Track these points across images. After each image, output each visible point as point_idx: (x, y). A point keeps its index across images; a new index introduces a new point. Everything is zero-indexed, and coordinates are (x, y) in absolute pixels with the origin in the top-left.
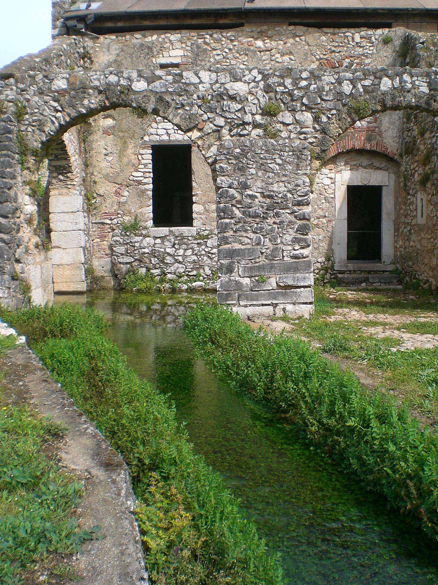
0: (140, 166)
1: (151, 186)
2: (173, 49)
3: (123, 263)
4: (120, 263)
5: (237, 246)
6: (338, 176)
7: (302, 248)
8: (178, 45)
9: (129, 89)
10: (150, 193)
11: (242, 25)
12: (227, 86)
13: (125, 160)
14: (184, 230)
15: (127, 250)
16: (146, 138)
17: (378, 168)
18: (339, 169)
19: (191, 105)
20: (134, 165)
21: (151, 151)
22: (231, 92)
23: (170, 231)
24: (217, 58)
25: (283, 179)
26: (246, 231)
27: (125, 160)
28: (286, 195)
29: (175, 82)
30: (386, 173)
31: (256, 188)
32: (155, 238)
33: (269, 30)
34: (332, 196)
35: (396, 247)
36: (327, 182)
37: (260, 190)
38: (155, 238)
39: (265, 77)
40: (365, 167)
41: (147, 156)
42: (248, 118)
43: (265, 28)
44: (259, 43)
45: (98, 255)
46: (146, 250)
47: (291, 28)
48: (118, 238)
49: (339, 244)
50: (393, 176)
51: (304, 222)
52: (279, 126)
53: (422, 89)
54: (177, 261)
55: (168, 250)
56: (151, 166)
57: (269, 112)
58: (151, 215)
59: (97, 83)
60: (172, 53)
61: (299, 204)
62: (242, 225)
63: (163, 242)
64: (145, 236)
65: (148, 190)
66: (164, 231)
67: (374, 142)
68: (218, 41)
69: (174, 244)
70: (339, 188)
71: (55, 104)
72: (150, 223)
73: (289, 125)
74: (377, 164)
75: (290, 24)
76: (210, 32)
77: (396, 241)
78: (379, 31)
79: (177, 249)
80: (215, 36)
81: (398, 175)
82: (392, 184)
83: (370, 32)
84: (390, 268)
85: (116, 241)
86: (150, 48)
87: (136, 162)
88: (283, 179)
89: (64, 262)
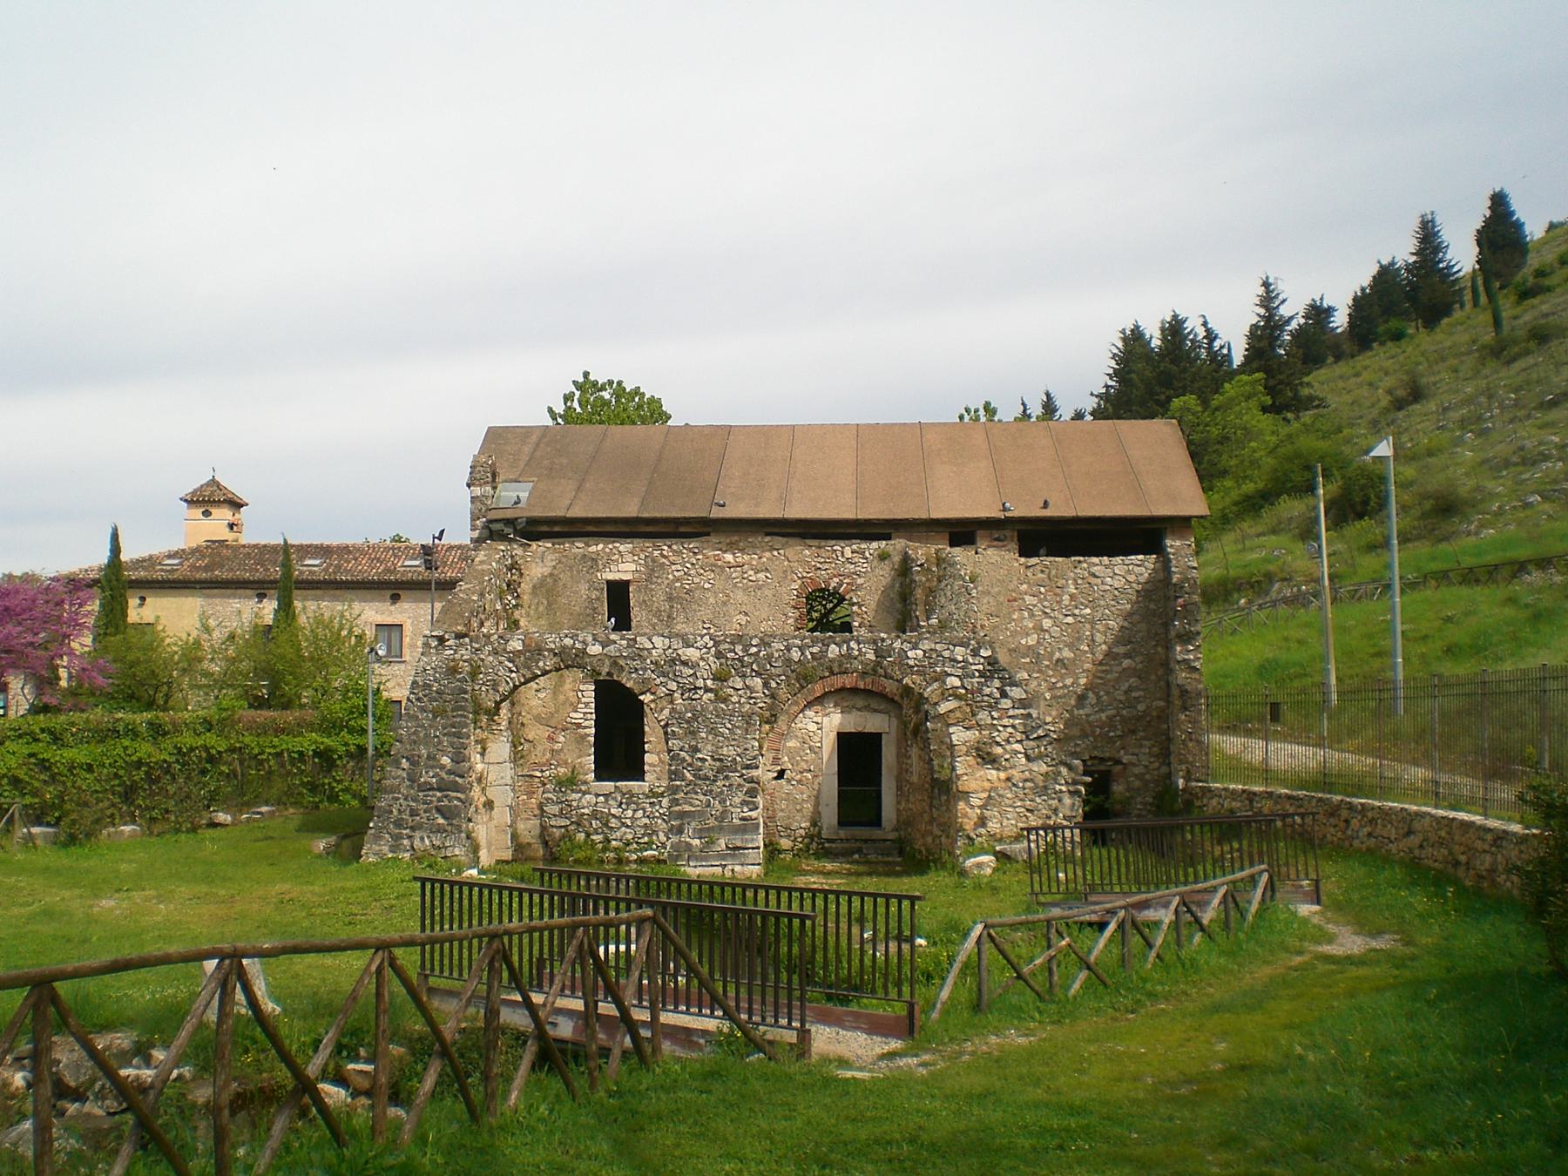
1: (593, 731)
5: (687, 808)
8: (629, 557)
9: (584, 652)
10: (592, 739)
11: (708, 534)
13: (562, 697)
17: (876, 711)
19: (645, 669)
27: (562, 697)
29: (629, 646)
30: (886, 717)
32: (597, 795)
38: (597, 795)
39: (716, 644)
41: (589, 692)
42: (700, 683)
44: (729, 557)
45: (524, 816)
46: (586, 811)
47: (767, 539)
50: (895, 722)
57: (720, 678)
61: (748, 767)
62: (692, 788)
64: (584, 793)
72: (592, 776)
74: (874, 705)
75: (767, 534)
77: (899, 803)
78: (875, 545)
81: (899, 717)
82: (894, 729)
84: (892, 836)
87: (575, 700)
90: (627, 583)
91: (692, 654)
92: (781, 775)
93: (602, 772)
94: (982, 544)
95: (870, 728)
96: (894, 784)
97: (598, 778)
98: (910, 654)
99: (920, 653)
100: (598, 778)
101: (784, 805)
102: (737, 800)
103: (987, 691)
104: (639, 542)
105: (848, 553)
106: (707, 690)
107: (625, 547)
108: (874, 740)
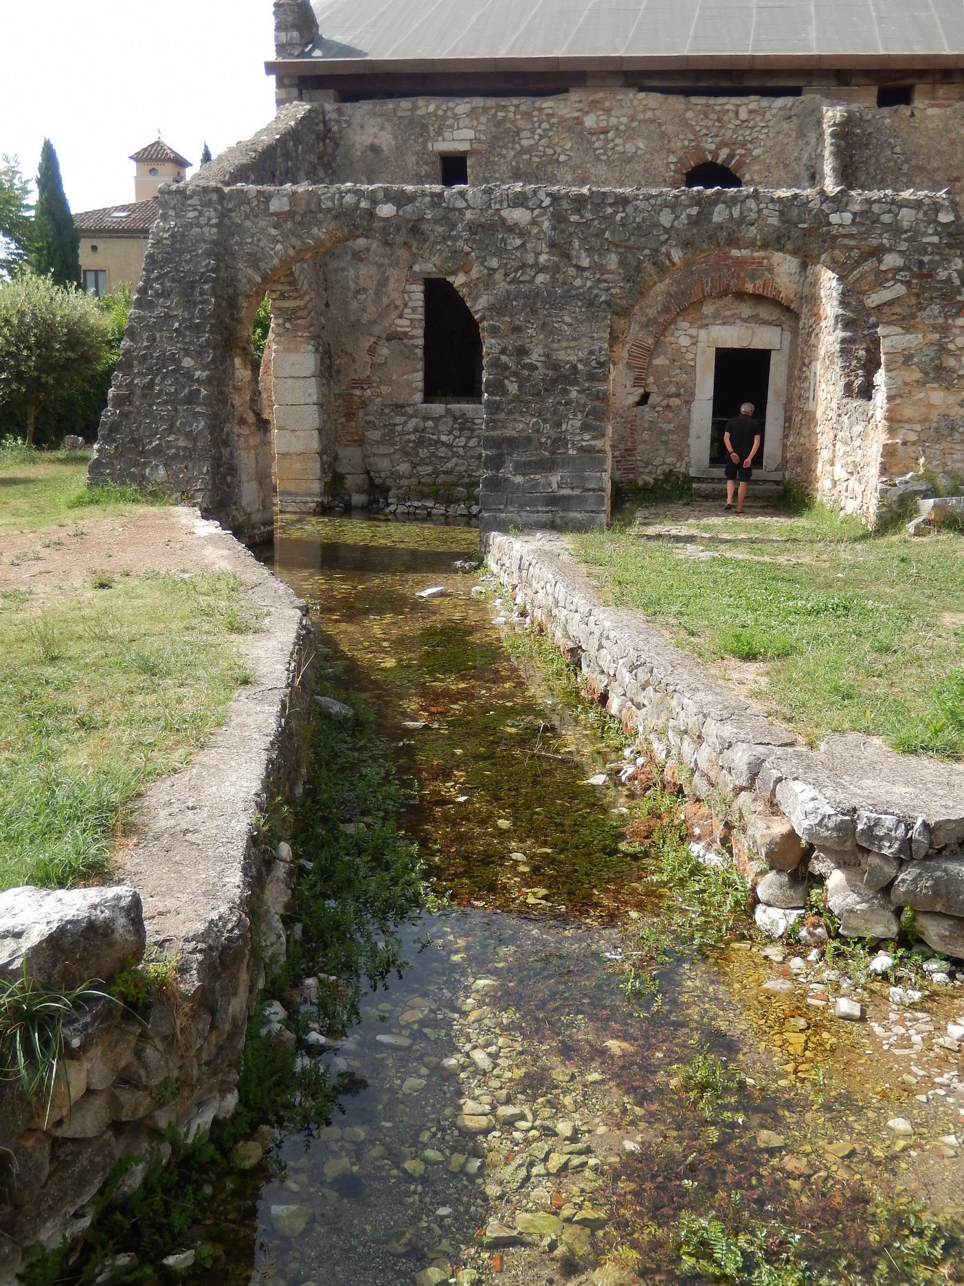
0: (407, 311)
1: (421, 342)
2: (458, 128)
3: (378, 455)
4: (375, 455)
6: (703, 333)
7: (594, 438)
8: (467, 121)
9: (371, 214)
10: (420, 352)
11: (566, 91)
12: (504, 213)
13: (385, 300)
14: (467, 408)
15: (383, 435)
16: (416, 268)
18: (705, 322)
19: (455, 239)
20: (397, 307)
21: (421, 288)
22: (510, 222)
23: (448, 410)
24: (525, 143)
25: (572, 344)
26: (521, 413)
27: (385, 300)
28: (575, 367)
29: (433, 205)
30: (778, 330)
31: (536, 356)
32: (426, 418)
33: (605, 99)
34: (692, 363)
35: (785, 446)
36: (684, 341)
37: (542, 359)
40: (745, 320)
41: (417, 294)
43: (599, 95)
46: (412, 437)
47: (642, 95)
48: (372, 418)
49: (699, 437)
50: (788, 336)
51: (598, 403)
52: (572, 271)
53: (770, 221)
54: (455, 454)
55: (444, 438)
56: (421, 310)
58: (421, 385)
59: (329, 204)
60: (458, 134)
63: (436, 426)
64: (411, 416)
65: (417, 347)
66: (438, 408)
67: (759, 282)
68: (527, 115)
69: (453, 429)
70: (704, 352)
71: (274, 232)
72: (419, 397)
73: (584, 269)
75: (642, 89)
76: (515, 101)
77: (786, 436)
78: (780, 102)
79: (456, 437)
80: (523, 108)
82: (787, 343)
83: (765, 102)
85: (368, 423)
86: (424, 127)
88: (572, 344)
89: (293, 450)
90: (465, 152)
91: (519, 216)
92: (644, 399)
93: (432, 392)
94: (919, 103)
95: (758, 344)
96: (781, 415)
97: (427, 400)
98: (834, 218)
99: (848, 217)
100: (426, 401)
101: (646, 435)
102: (578, 424)
103: (942, 274)
104: (478, 102)
105: (743, 115)
106: (543, 269)
107: (462, 106)
108: (760, 359)
